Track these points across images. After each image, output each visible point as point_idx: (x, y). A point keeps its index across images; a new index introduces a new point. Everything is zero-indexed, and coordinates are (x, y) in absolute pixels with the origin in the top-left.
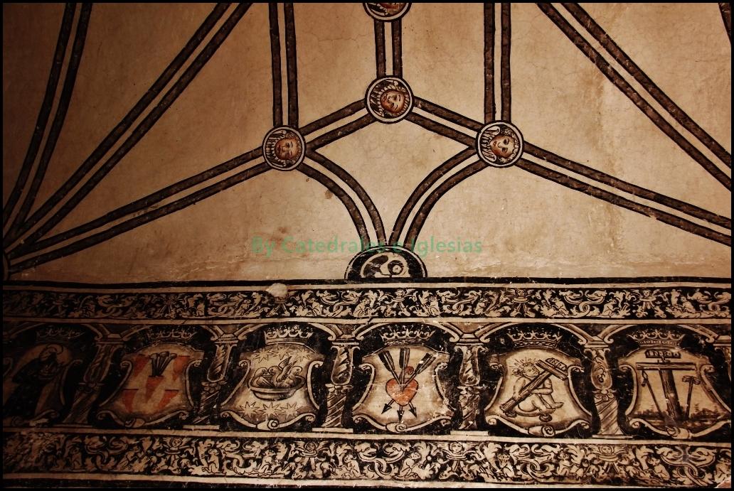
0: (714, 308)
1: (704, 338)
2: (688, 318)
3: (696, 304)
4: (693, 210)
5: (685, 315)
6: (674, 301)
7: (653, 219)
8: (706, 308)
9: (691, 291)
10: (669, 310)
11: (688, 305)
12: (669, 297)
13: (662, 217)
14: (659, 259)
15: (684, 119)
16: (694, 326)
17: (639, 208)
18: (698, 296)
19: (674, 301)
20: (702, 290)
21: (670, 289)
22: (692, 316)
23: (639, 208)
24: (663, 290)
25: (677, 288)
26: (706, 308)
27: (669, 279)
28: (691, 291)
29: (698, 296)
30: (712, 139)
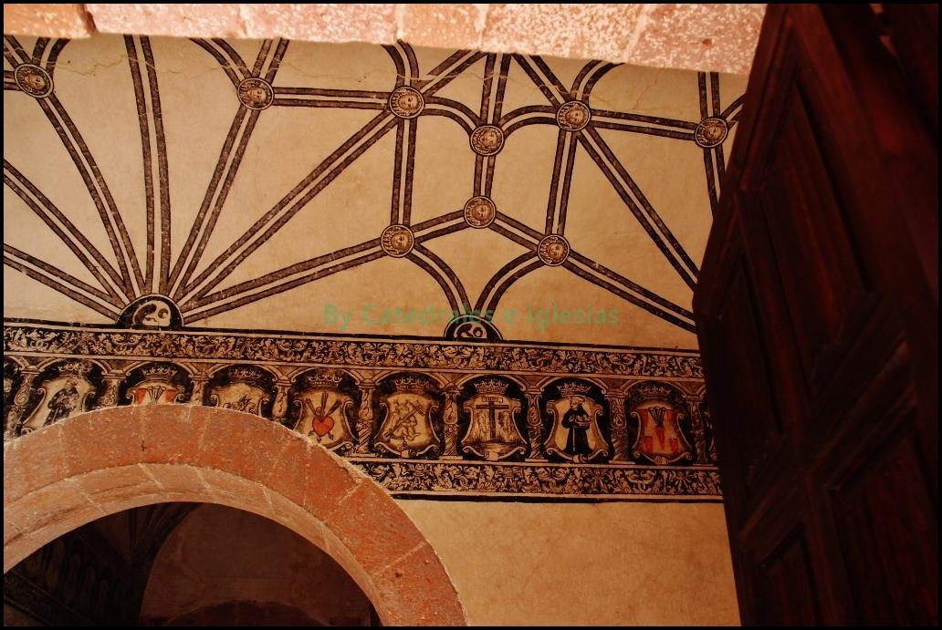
0: (40, 344)
1: (20, 366)
2: (18, 351)
3: (29, 340)
4: (52, 269)
5: (19, 348)
6: (17, 337)
7: (24, 274)
8: (34, 344)
9: (30, 330)
10: (9, 344)
11: (24, 341)
12: (15, 334)
13: (32, 274)
14: (20, 304)
15: (48, 203)
16: (18, 357)
17: (16, 265)
18: (34, 335)
19: (17, 337)
20: (39, 330)
21: (17, 328)
22: (22, 349)
23: (16, 265)
24: (13, 328)
25: (22, 328)
26: (34, 344)
27: (21, 321)
28: (30, 330)
29: (34, 335)
30: (67, 220)
